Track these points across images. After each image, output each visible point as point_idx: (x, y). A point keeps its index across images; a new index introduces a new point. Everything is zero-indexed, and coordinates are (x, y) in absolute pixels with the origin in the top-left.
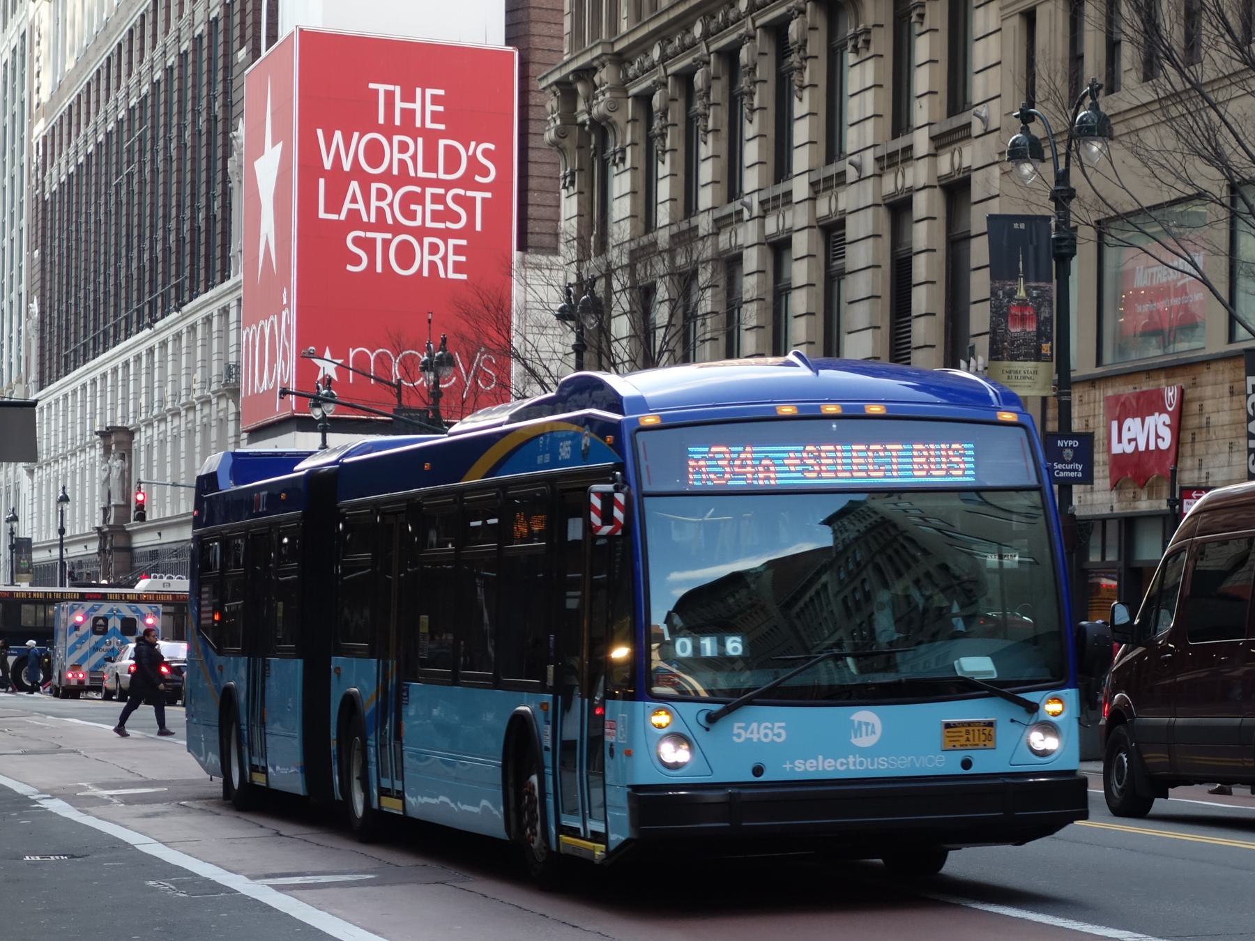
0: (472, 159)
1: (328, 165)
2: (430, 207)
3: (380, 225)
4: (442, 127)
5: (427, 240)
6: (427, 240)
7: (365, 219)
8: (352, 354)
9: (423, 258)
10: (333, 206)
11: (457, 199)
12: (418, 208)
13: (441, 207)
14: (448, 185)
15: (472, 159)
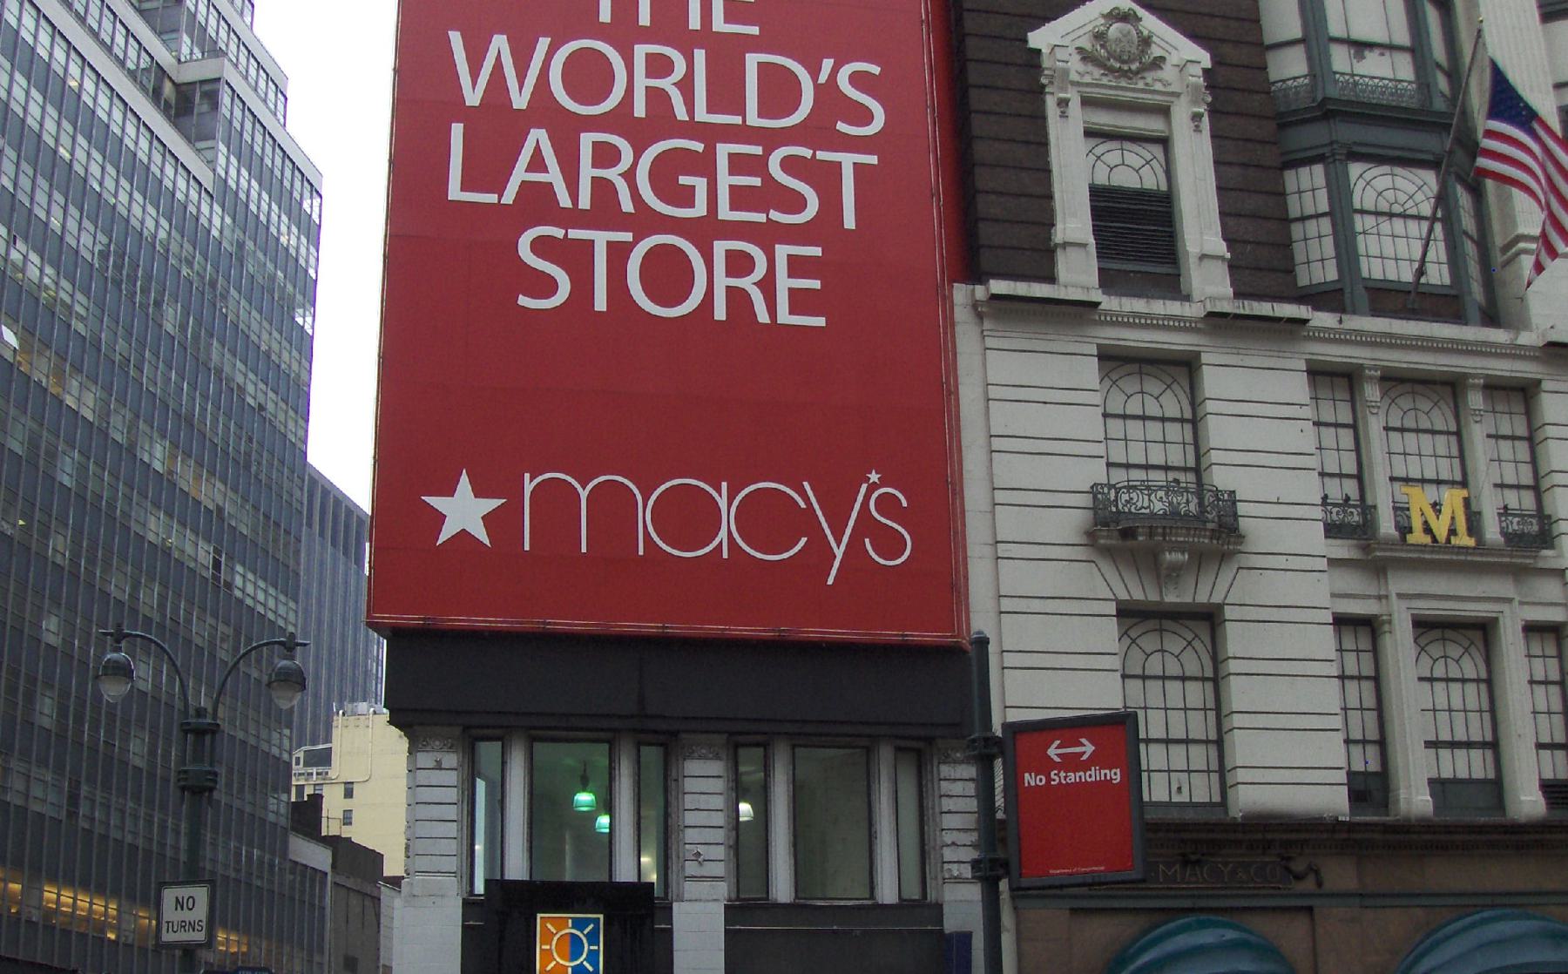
1: (473, 97)
2: (725, 180)
4: (754, 30)
5: (720, 248)
6: (720, 248)
7: (565, 201)
8: (529, 487)
9: (711, 283)
11: (789, 164)
12: (700, 184)
13: (756, 181)
14: (771, 139)
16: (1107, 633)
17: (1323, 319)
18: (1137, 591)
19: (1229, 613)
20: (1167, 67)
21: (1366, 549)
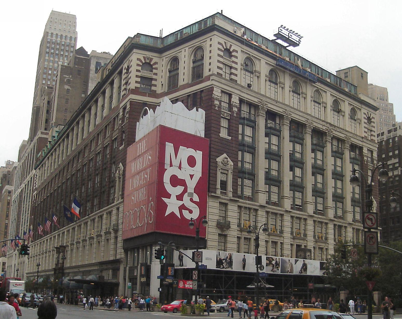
16: (217, 237)
17: (241, 200)
19: (228, 235)
20: (229, 165)
21: (240, 229)
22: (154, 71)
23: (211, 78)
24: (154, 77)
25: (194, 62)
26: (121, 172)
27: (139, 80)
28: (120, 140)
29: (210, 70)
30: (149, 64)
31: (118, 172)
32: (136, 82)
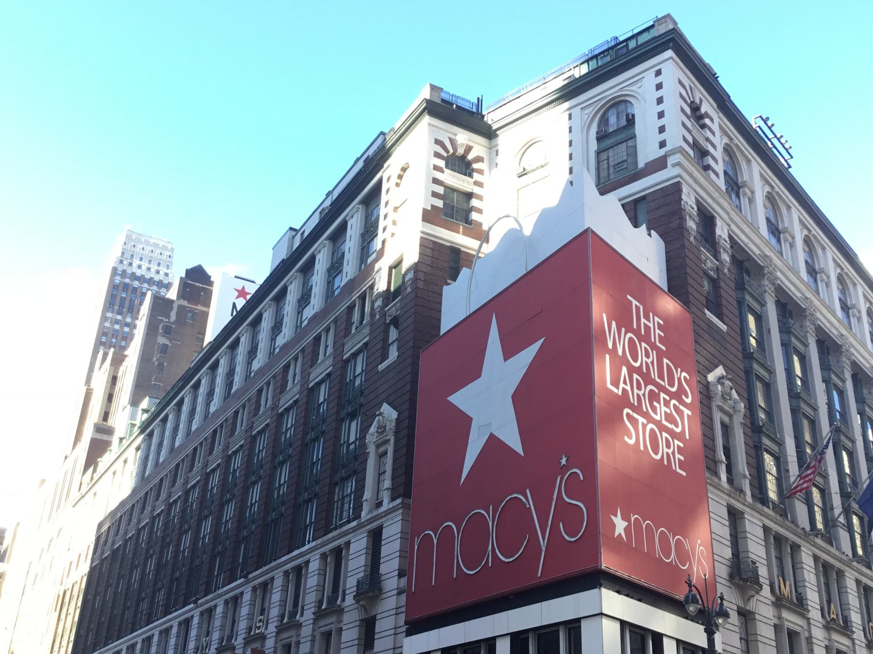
0: (679, 379)
1: (610, 346)
3: (638, 409)
5: (665, 435)
10: (616, 384)
13: (668, 411)
14: (672, 395)
15: (679, 379)
18: (741, 604)
19: (757, 617)
22: (476, 176)
23: (671, 161)
24: (476, 190)
25: (600, 139)
26: (391, 426)
27: (440, 190)
28: (380, 345)
29: (662, 144)
30: (463, 157)
31: (373, 429)
32: (435, 195)
